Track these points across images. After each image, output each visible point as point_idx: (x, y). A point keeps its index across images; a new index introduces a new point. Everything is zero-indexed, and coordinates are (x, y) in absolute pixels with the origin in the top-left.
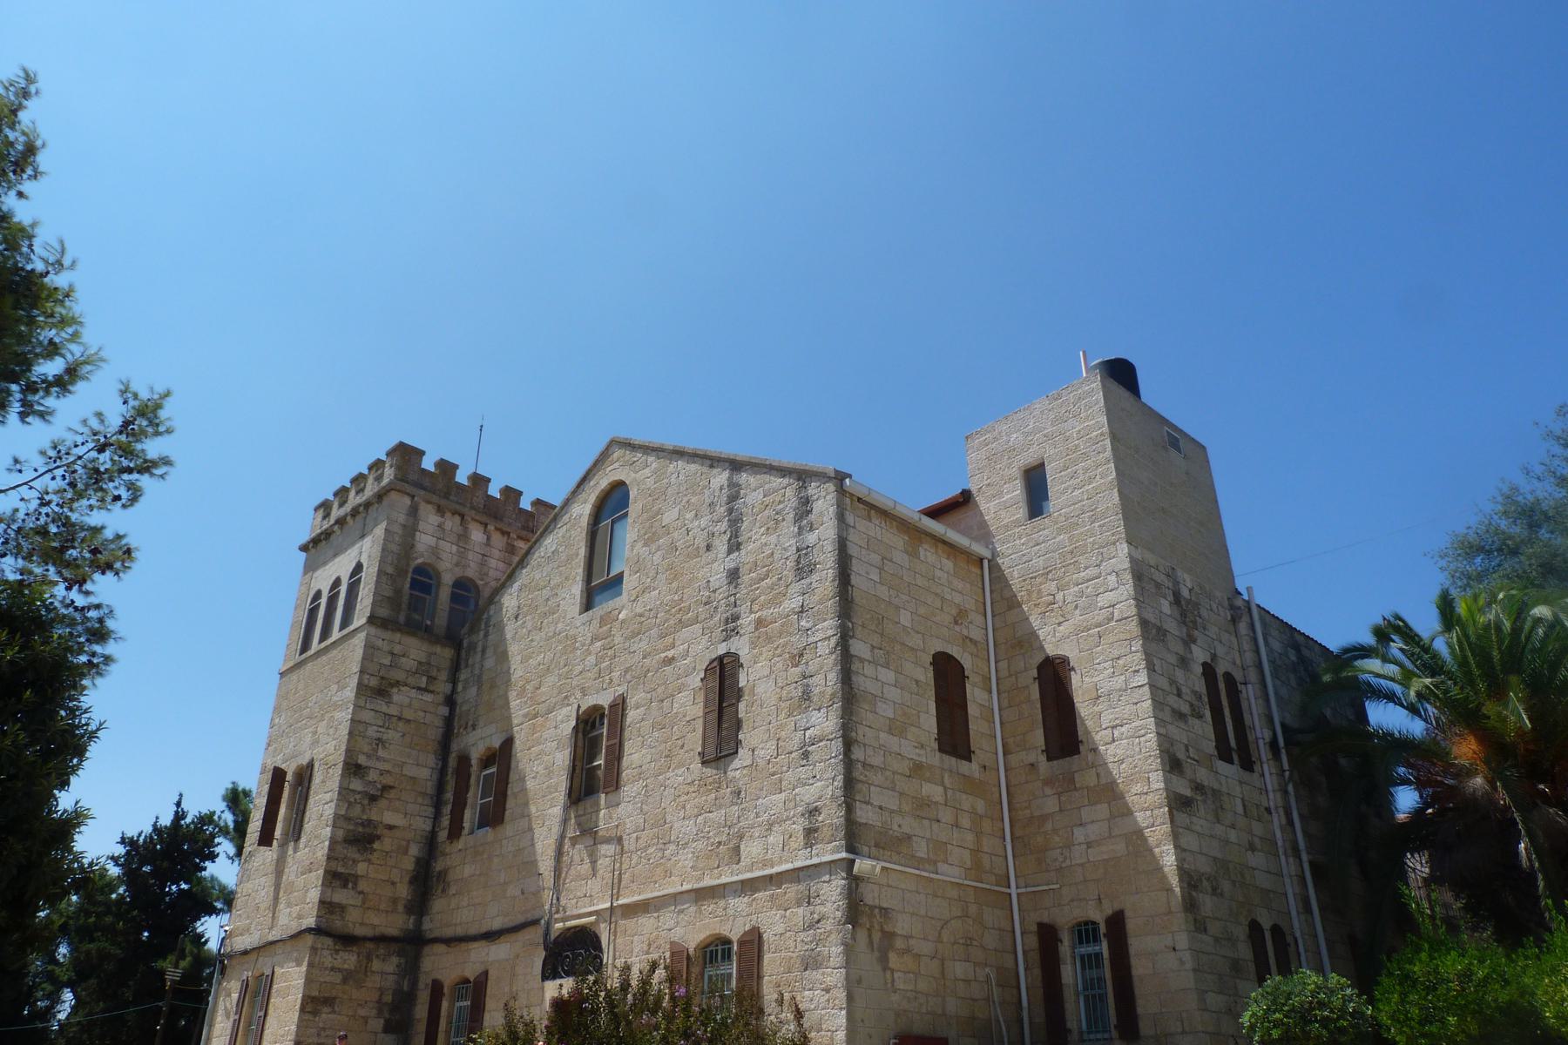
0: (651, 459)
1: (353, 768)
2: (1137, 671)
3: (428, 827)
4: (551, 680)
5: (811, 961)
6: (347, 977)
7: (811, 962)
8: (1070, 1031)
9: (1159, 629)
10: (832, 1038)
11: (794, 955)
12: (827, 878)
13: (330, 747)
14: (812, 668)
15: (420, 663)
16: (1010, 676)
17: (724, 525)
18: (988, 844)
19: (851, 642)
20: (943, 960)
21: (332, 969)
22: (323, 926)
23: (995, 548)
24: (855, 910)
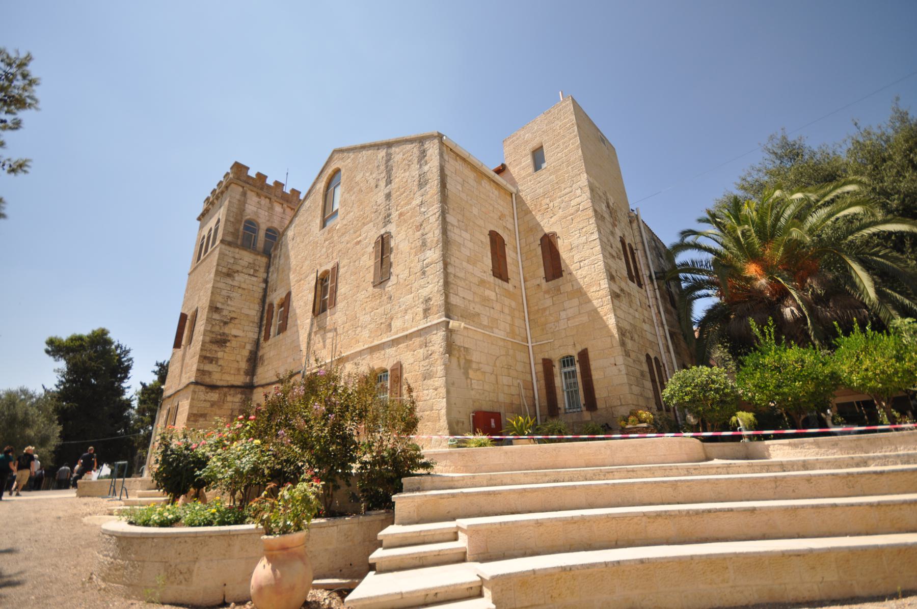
0: (351, 154)
1: (214, 309)
2: (593, 233)
3: (256, 337)
4: (307, 262)
5: (427, 375)
6: (213, 404)
7: (427, 376)
8: (560, 408)
9: (602, 216)
10: (439, 414)
11: (418, 373)
12: (435, 332)
13: (204, 301)
14: (426, 230)
15: (250, 263)
16: (527, 245)
17: (384, 174)
18: (517, 322)
19: (447, 215)
20: (496, 375)
21: (205, 401)
22: (199, 381)
23: (518, 188)
24: (450, 348)
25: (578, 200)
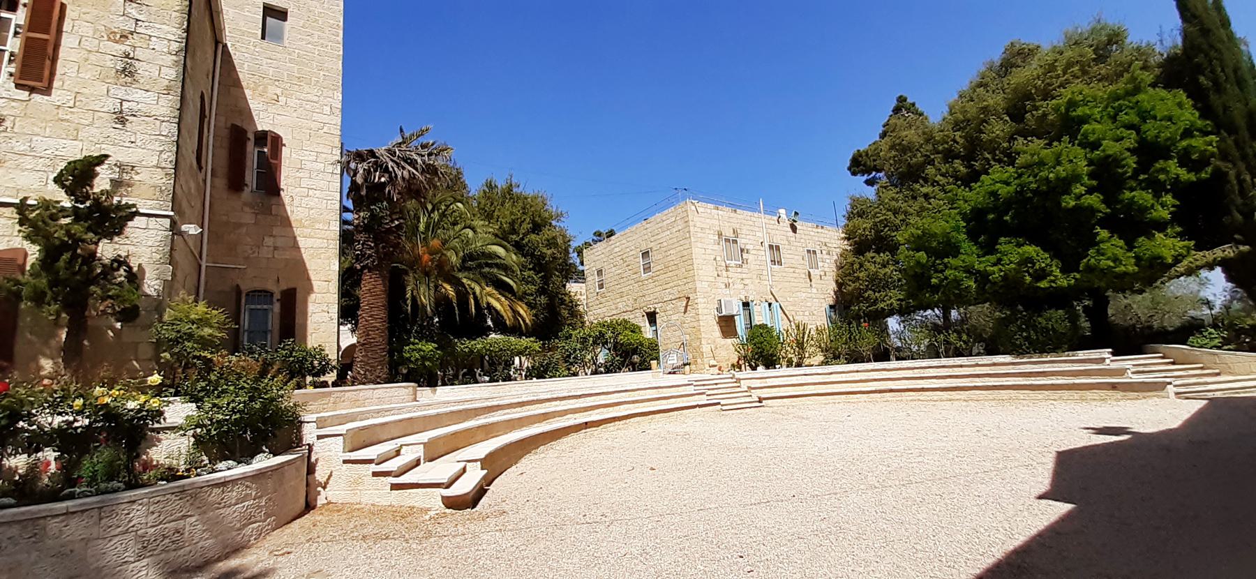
25: (326, 119)
